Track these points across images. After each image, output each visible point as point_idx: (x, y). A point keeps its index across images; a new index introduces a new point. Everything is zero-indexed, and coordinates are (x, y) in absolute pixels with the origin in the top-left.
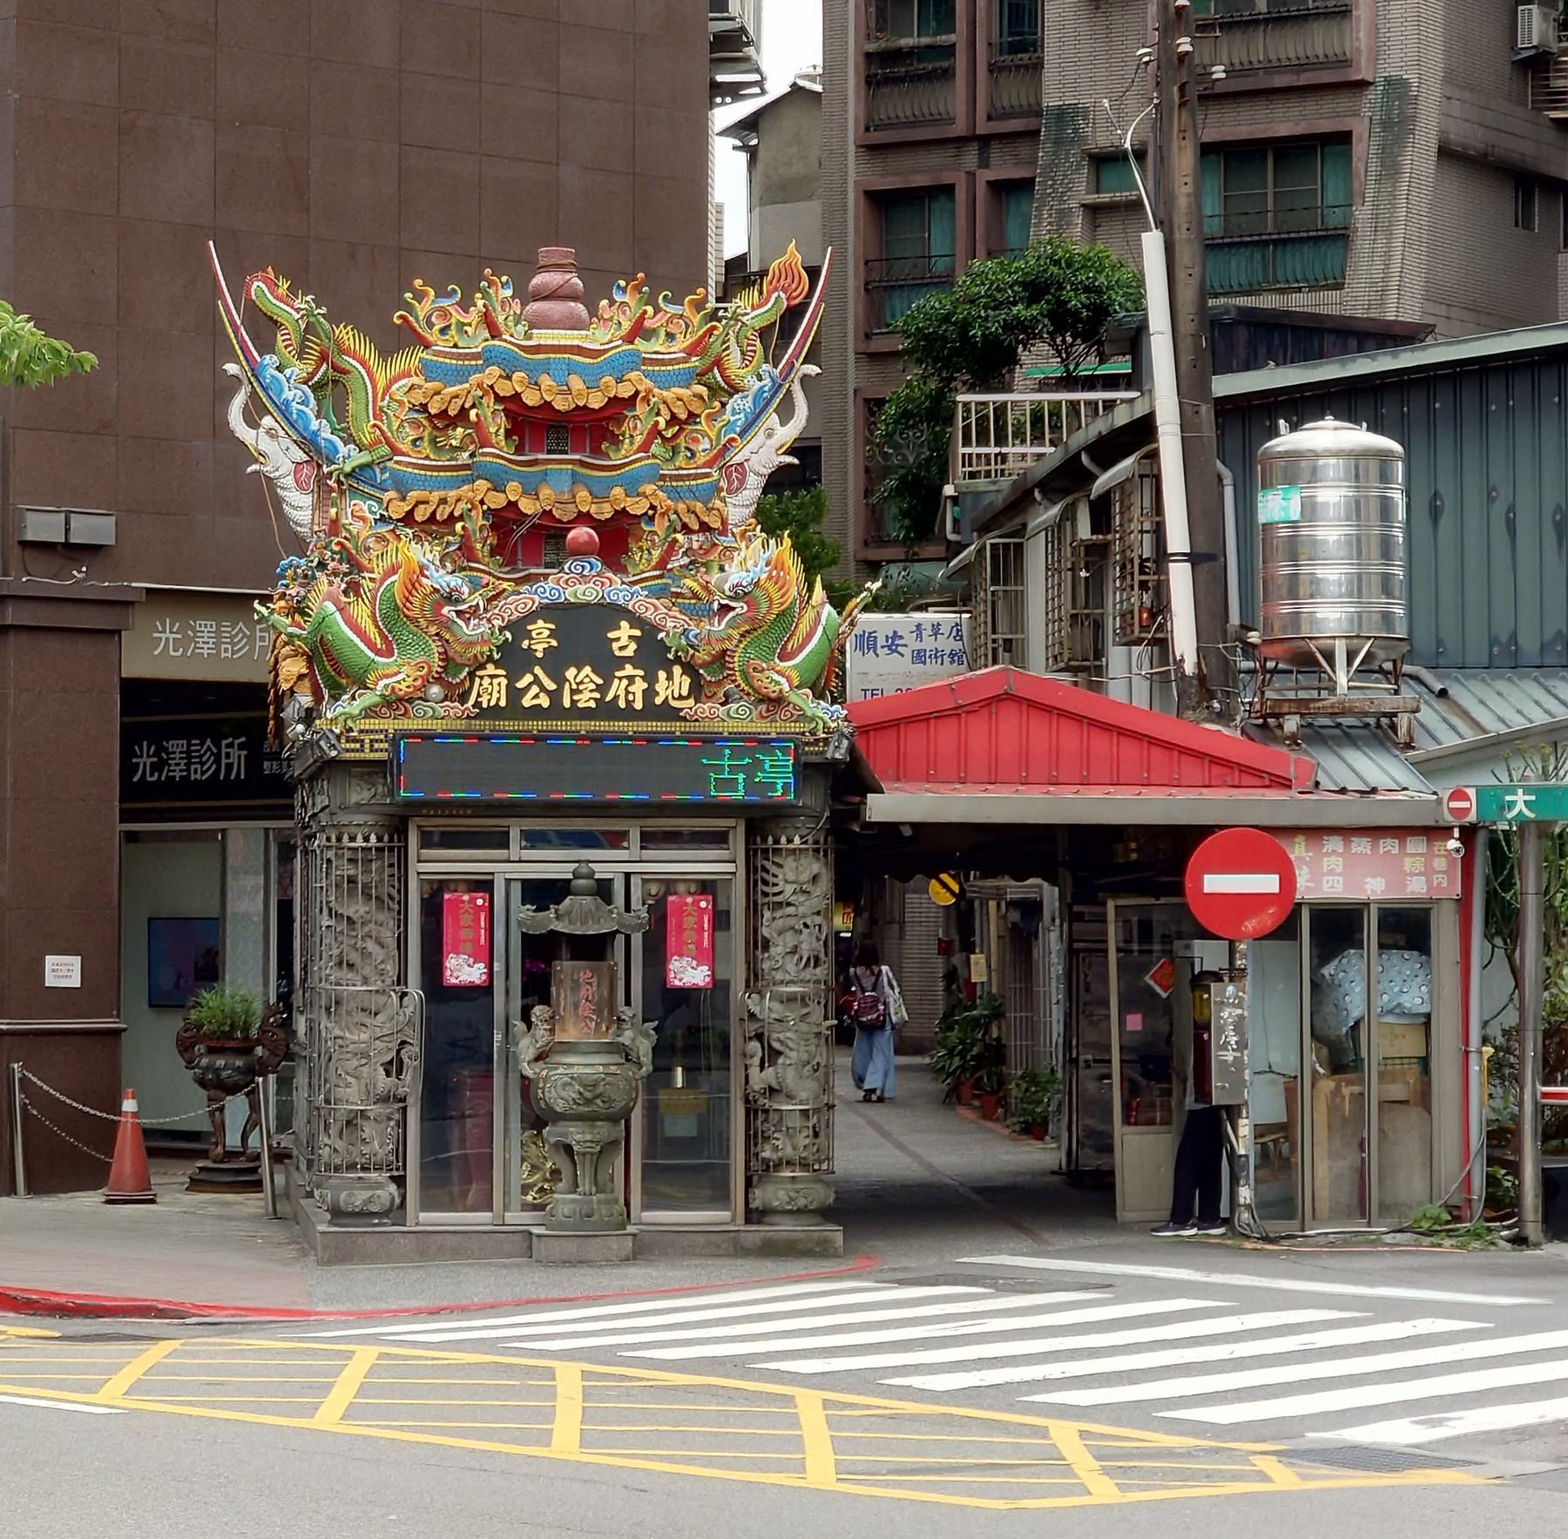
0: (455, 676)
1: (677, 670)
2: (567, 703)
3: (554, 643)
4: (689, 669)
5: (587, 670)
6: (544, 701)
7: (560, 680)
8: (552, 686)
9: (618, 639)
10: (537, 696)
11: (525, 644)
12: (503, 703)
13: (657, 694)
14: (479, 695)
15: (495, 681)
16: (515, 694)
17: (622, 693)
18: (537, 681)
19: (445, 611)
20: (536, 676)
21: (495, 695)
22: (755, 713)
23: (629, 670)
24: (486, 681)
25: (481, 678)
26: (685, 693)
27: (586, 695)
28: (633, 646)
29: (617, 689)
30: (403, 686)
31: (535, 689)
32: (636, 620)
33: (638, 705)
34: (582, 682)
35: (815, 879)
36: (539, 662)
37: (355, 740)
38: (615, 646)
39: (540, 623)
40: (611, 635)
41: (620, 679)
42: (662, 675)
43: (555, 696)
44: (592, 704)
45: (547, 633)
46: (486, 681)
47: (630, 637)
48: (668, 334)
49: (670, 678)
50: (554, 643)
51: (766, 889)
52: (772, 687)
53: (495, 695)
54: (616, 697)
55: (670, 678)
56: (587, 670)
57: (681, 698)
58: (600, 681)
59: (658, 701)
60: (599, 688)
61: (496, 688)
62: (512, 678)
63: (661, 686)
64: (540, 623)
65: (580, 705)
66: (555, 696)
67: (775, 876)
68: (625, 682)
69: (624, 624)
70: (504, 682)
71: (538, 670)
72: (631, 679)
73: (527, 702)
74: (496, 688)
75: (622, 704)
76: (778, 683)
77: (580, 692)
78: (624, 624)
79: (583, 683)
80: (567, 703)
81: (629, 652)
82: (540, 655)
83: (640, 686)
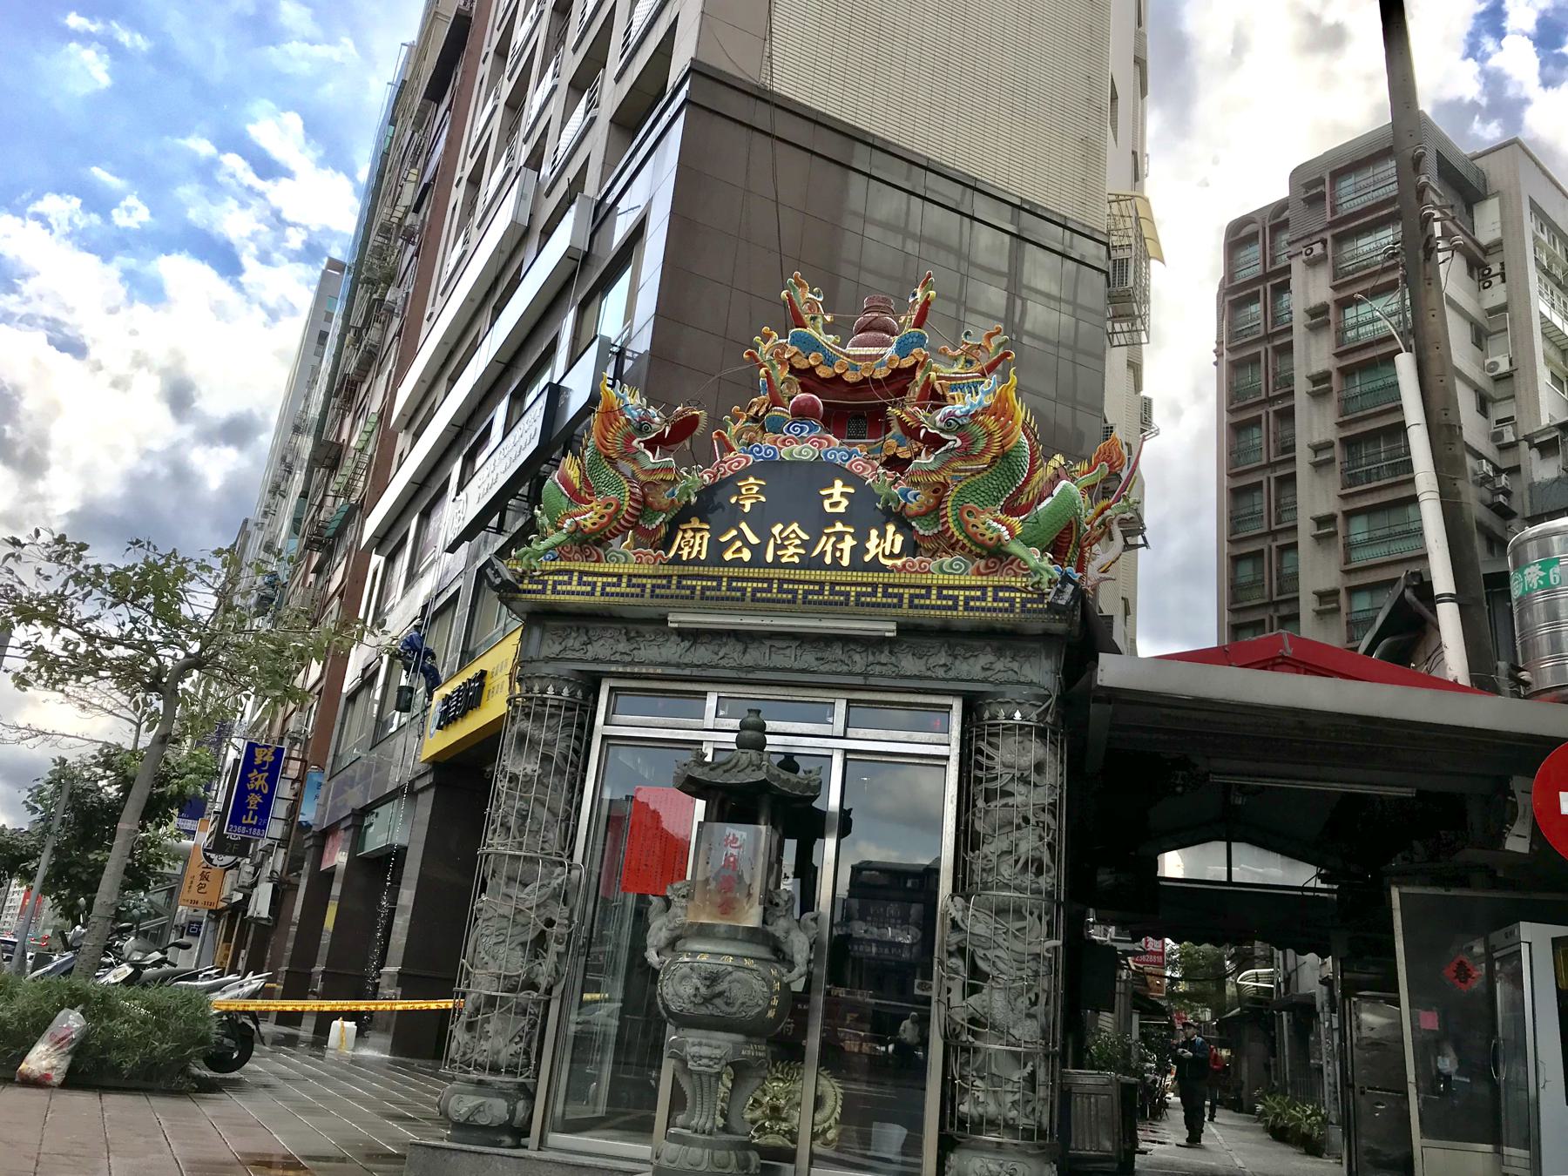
0: (651, 521)
1: (891, 528)
2: (769, 558)
3: (763, 499)
4: (903, 525)
5: (795, 526)
6: (746, 555)
7: (765, 535)
8: (754, 540)
9: (830, 496)
10: (739, 550)
11: (733, 500)
12: (703, 557)
13: (867, 551)
14: (680, 548)
15: (698, 536)
16: (717, 548)
17: (829, 548)
18: (741, 536)
19: (635, 443)
20: (741, 531)
21: (696, 548)
22: (971, 568)
23: (839, 527)
24: (690, 534)
25: (685, 531)
26: (897, 550)
27: (791, 550)
28: (845, 502)
29: (825, 545)
30: (588, 524)
31: (738, 544)
32: (850, 478)
33: (845, 562)
34: (787, 538)
35: (1039, 767)
36: (745, 517)
37: (537, 583)
38: (827, 503)
39: (752, 480)
40: (823, 492)
41: (828, 536)
42: (874, 533)
43: (758, 551)
44: (796, 560)
45: (756, 488)
46: (690, 534)
47: (842, 494)
48: (967, 361)
49: (882, 536)
50: (763, 499)
51: (979, 774)
52: (989, 534)
53: (696, 548)
54: (823, 553)
55: (882, 536)
56: (795, 526)
57: (892, 556)
58: (806, 537)
59: (867, 558)
60: (804, 544)
61: (698, 541)
62: (716, 533)
63: (872, 544)
64: (752, 480)
65: (784, 560)
66: (758, 551)
67: (989, 757)
68: (833, 539)
69: (838, 483)
70: (707, 535)
71: (743, 526)
72: (840, 537)
73: (728, 556)
74: (698, 541)
75: (828, 560)
76: (995, 530)
77: (785, 547)
78: (838, 483)
79: (789, 539)
80: (769, 558)
81: (841, 509)
82: (747, 509)
83: (849, 542)
